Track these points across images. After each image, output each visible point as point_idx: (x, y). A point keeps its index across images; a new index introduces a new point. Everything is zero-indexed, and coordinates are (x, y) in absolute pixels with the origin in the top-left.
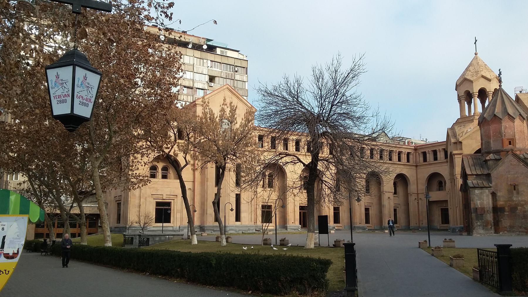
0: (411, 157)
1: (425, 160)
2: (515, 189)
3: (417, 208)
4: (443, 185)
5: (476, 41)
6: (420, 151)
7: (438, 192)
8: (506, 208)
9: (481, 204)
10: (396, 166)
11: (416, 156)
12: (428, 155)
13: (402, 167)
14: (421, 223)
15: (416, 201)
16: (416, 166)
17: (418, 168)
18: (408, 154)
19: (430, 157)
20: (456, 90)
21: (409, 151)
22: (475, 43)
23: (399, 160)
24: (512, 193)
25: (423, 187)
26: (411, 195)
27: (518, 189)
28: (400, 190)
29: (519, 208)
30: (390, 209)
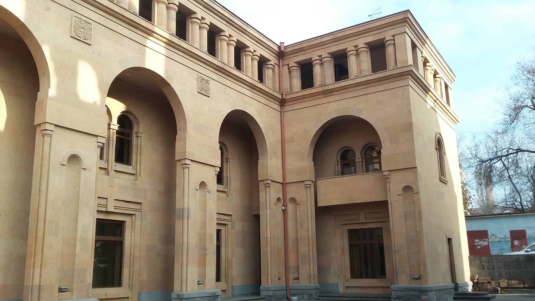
0: (268, 73)
3: (281, 230)
6: (292, 61)
7: (346, 179)
10: (229, 82)
11: (280, 76)
12: (317, 70)
14: (292, 276)
15: (280, 207)
16: (282, 103)
17: (286, 108)
19: (324, 74)
25: (301, 163)
26: (267, 186)
28: (234, 173)
30: (204, 226)
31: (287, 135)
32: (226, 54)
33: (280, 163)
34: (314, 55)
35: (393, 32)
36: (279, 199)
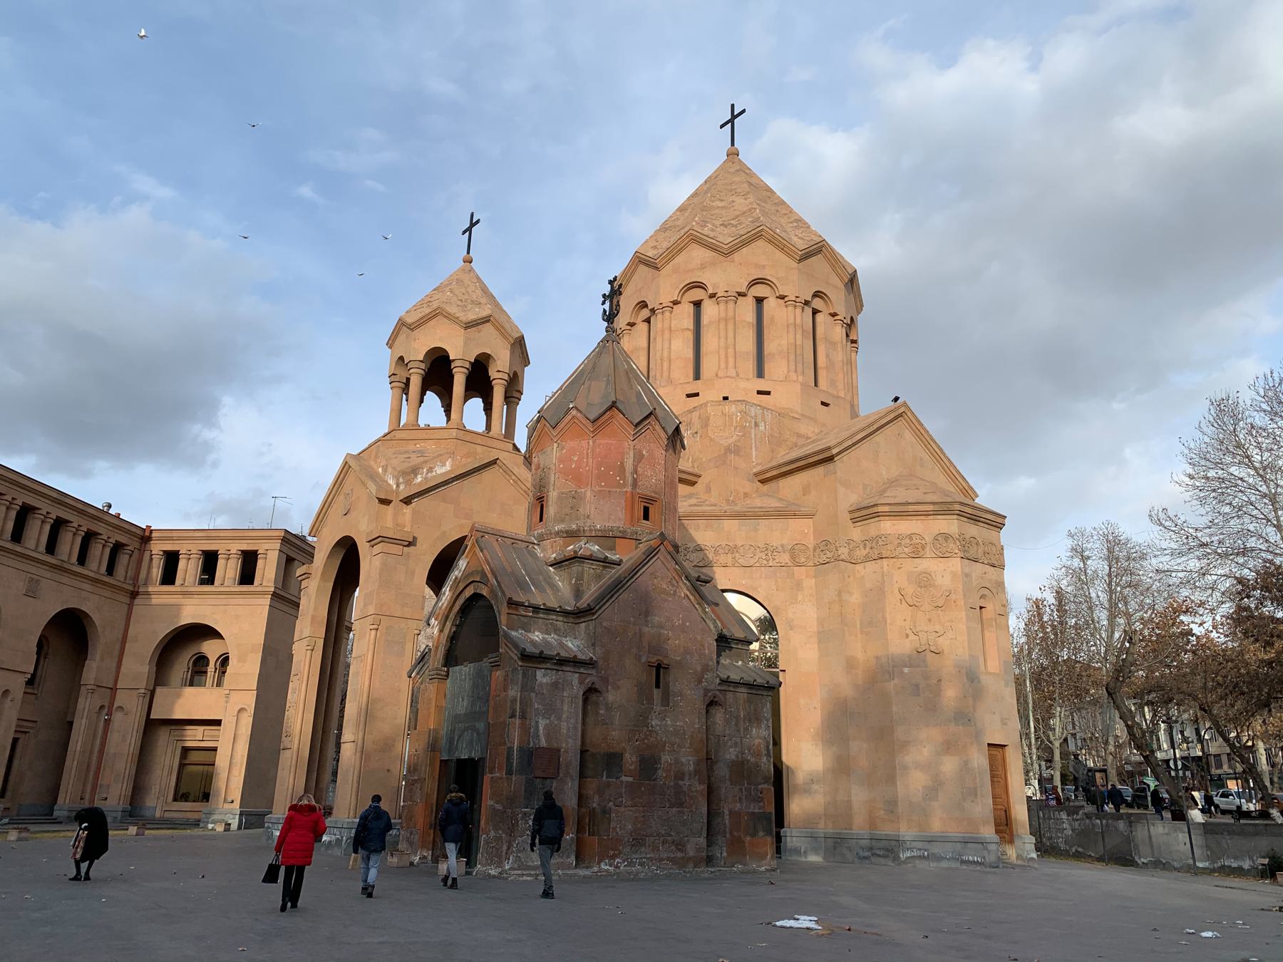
0: (123, 559)
1: (169, 576)
2: (658, 686)
4: (211, 668)
5: (473, 225)
8: (627, 756)
9: (552, 732)
10: (64, 580)
12: (182, 564)
13: (87, 586)
17: (136, 601)
18: (117, 548)
20: (391, 344)
21: (123, 539)
22: (469, 230)
23: (82, 560)
24: (650, 699)
27: (667, 685)
29: (666, 758)
31: (131, 632)
32: (69, 545)
33: (114, 665)
34: (182, 548)
35: (267, 546)
36: (102, 707)
